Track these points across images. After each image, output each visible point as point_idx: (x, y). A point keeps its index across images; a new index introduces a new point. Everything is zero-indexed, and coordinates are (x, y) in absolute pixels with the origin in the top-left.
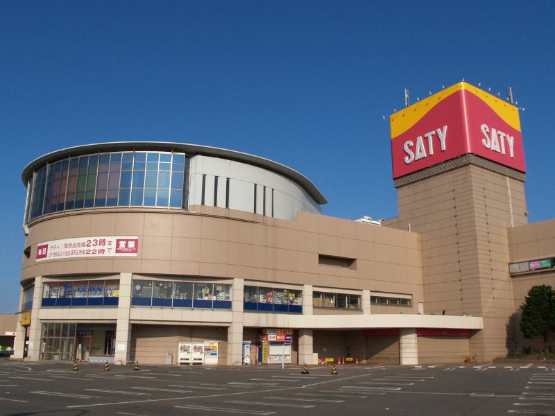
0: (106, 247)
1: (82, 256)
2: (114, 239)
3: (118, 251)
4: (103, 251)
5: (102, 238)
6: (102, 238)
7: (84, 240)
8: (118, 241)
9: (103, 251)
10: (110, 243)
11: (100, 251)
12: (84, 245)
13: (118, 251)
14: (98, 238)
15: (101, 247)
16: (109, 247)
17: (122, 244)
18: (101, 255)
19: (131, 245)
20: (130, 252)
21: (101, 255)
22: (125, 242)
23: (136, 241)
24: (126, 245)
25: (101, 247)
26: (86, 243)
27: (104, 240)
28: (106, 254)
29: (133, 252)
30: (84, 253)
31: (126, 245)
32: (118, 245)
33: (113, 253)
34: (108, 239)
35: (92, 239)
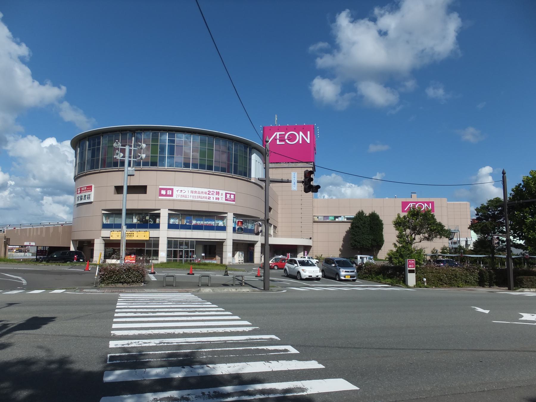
0: (220, 197)
1: (205, 200)
2: (224, 192)
3: (226, 200)
4: (218, 199)
5: (218, 191)
6: (218, 191)
7: (206, 190)
8: (226, 194)
9: (218, 199)
10: (222, 195)
11: (216, 199)
12: (206, 193)
13: (226, 200)
14: (215, 191)
15: (217, 196)
16: (222, 197)
17: (228, 196)
18: (217, 201)
19: (232, 197)
20: (232, 201)
21: (217, 201)
22: (229, 195)
23: (234, 195)
24: (230, 196)
25: (217, 196)
26: (208, 193)
27: (219, 192)
28: (220, 201)
29: (234, 201)
30: (206, 198)
31: (230, 196)
32: (226, 196)
33: (224, 201)
34: (221, 192)
35: (211, 190)
